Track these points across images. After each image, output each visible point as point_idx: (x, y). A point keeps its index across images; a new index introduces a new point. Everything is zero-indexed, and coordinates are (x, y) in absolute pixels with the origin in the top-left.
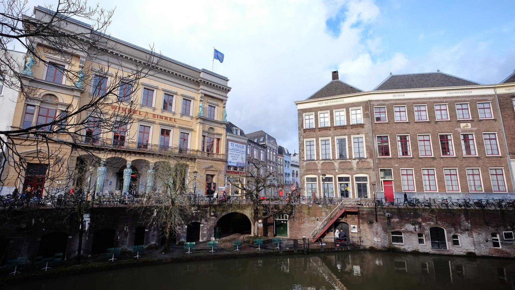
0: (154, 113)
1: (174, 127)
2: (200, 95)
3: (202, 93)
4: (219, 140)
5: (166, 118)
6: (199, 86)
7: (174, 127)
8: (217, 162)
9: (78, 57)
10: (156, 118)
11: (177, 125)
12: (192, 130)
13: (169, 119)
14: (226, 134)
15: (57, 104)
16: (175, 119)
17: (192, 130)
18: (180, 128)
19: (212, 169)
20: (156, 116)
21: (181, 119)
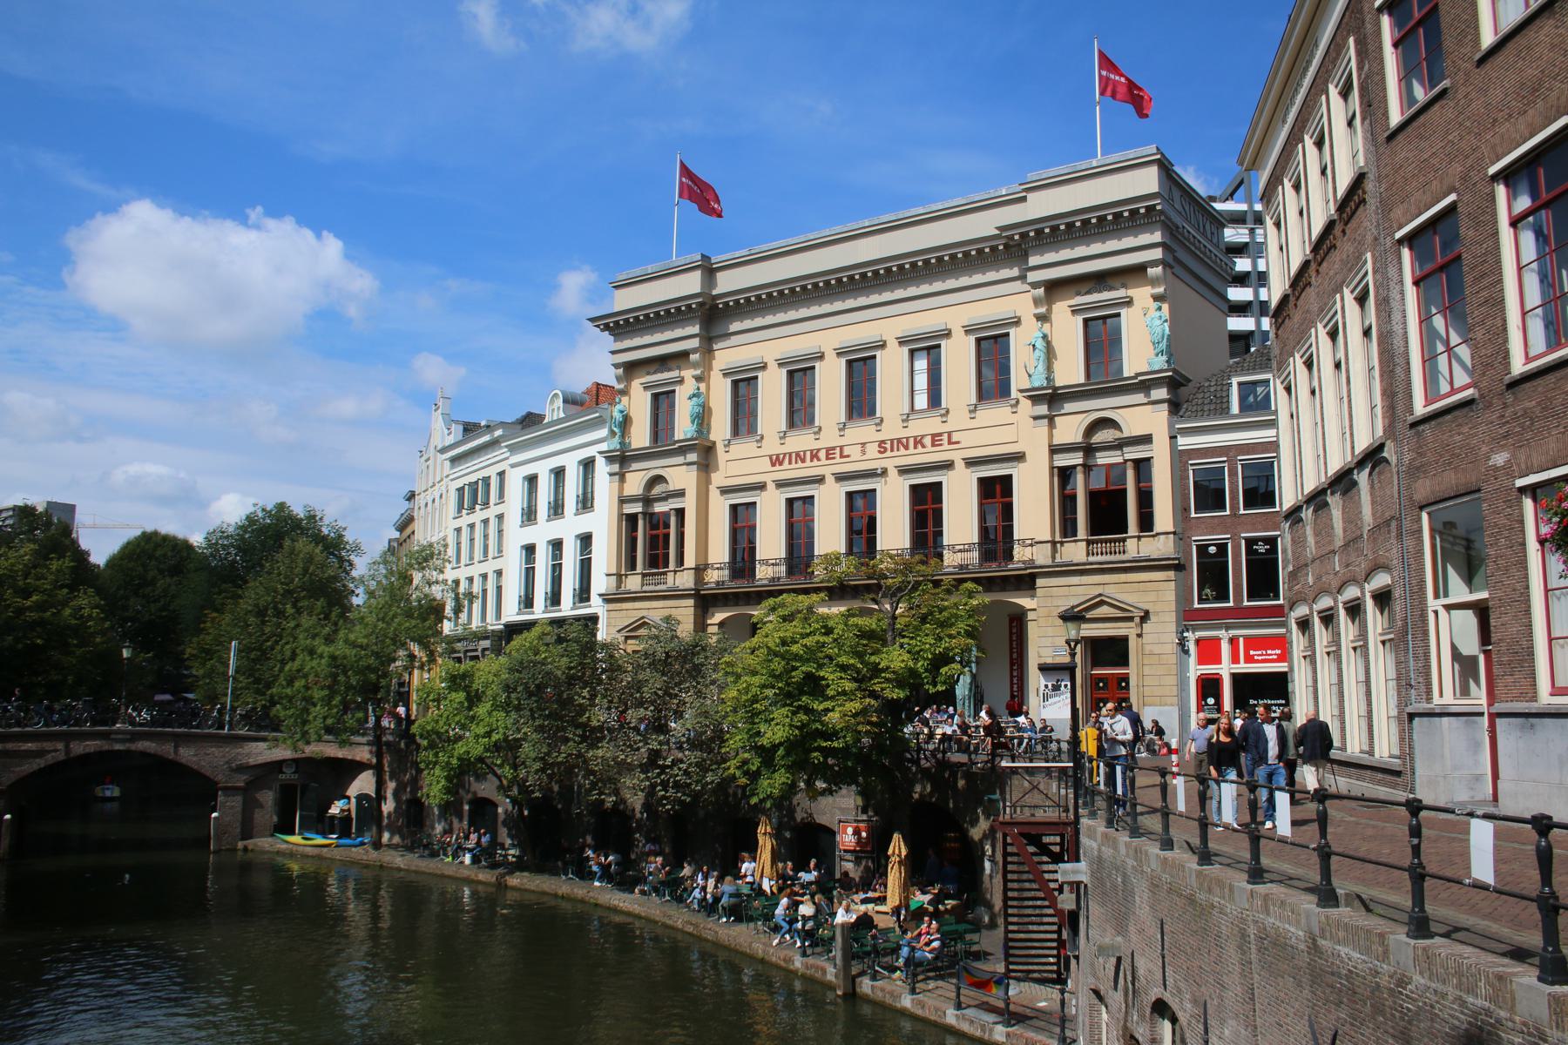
0: (881, 437)
1: (948, 465)
2: (1028, 298)
3: (1035, 285)
4: (1143, 466)
5: (918, 442)
6: (1026, 256)
7: (948, 465)
8: (1123, 577)
9: (684, 355)
10: (888, 454)
11: (957, 457)
12: (1019, 457)
13: (927, 441)
14: (1171, 426)
15: (665, 499)
16: (950, 434)
17: (1019, 457)
18: (971, 463)
19: (1104, 611)
20: (888, 446)
21: (974, 424)
